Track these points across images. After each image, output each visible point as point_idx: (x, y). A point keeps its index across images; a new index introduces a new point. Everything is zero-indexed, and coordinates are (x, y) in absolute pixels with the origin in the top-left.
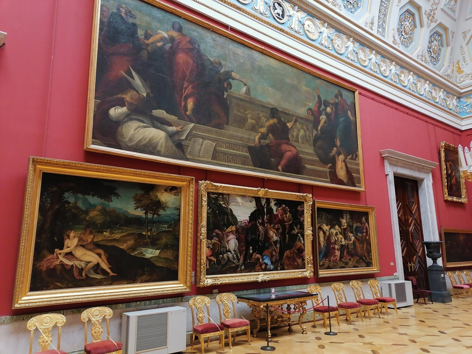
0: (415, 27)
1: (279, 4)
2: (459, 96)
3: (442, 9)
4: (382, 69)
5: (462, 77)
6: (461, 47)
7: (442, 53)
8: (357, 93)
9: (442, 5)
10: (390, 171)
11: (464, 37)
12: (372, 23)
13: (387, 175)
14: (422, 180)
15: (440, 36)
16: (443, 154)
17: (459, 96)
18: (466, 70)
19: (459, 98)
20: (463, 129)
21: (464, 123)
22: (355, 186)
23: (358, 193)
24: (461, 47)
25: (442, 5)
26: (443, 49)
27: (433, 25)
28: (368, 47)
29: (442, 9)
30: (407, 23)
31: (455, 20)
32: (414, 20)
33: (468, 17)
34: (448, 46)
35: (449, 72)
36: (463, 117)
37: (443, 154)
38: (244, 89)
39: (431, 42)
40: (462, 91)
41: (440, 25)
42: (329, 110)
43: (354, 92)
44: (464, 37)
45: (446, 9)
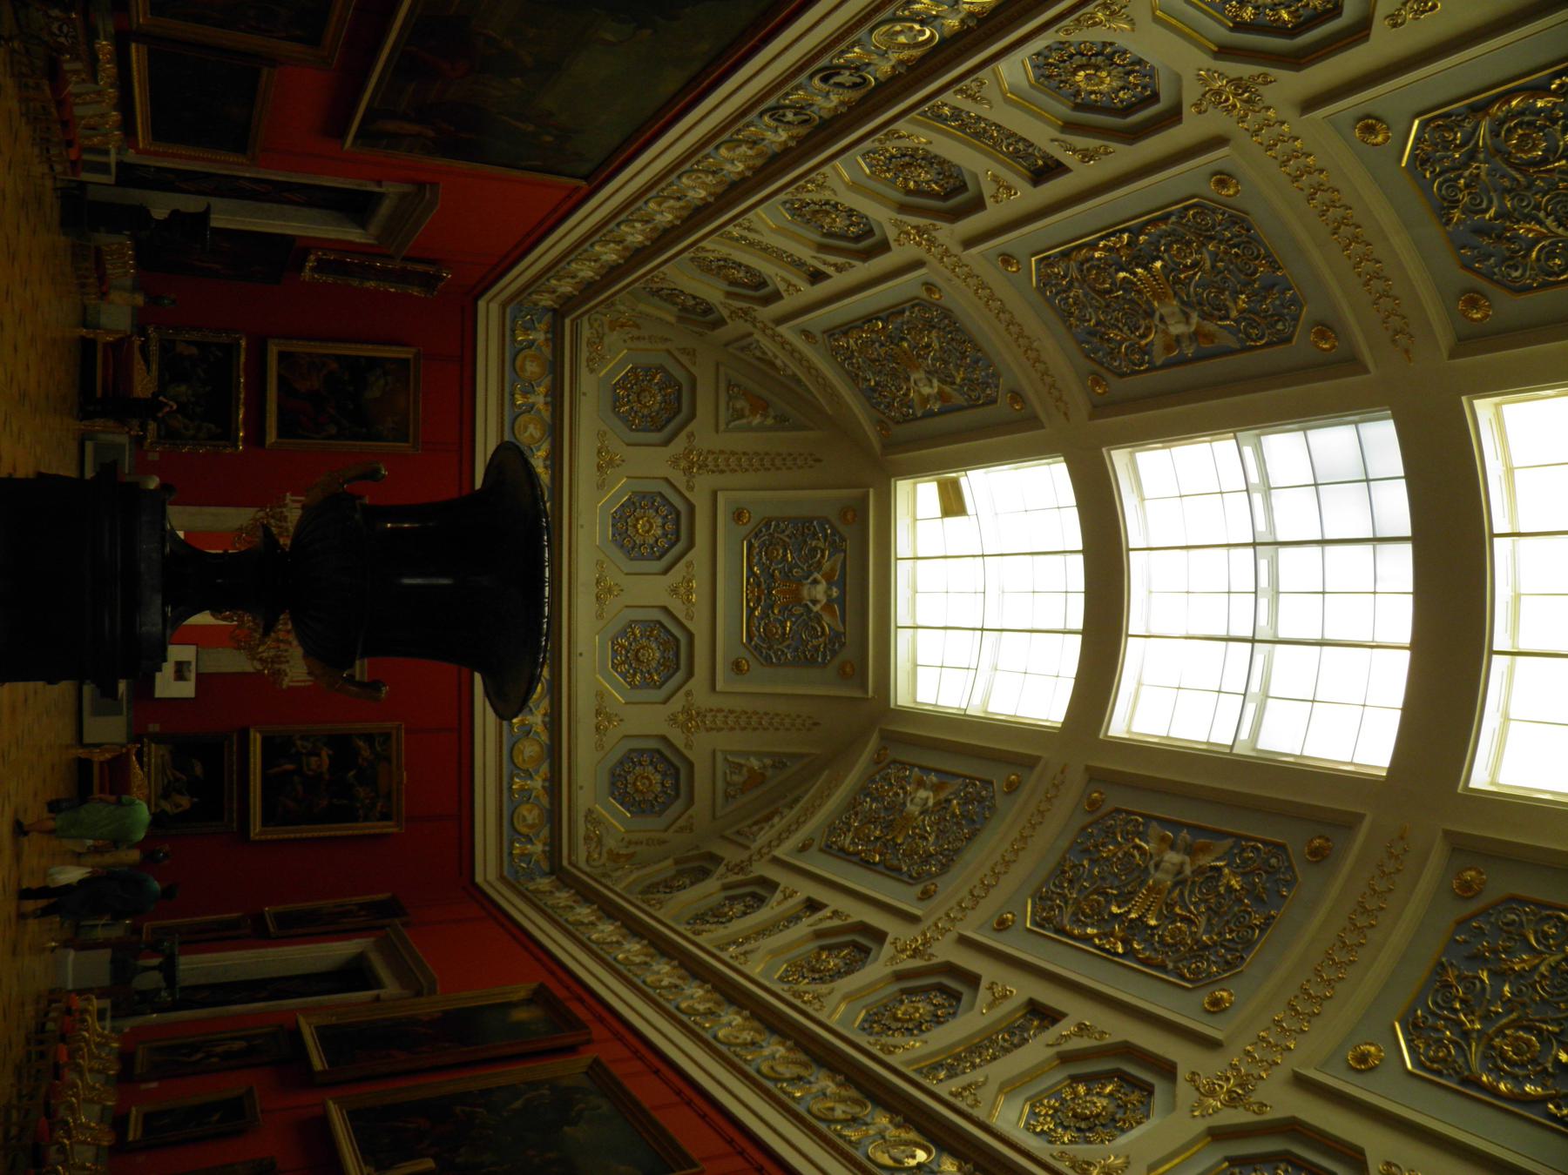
0: (733, 283)
1: (805, 122)
2: (558, 314)
3: (750, 334)
4: (638, 225)
5: (602, 325)
6: (666, 340)
7: (669, 306)
8: (583, 183)
9: (757, 336)
10: (391, 189)
11: (684, 351)
12: (749, 229)
13: (379, 183)
14: (363, 225)
15: (700, 315)
16: (420, 268)
17: (558, 314)
18: (613, 338)
19: (554, 310)
20: (481, 304)
21: (494, 307)
22: (356, 137)
23: (342, 135)
24: (666, 340)
25: (757, 336)
26: (675, 309)
27: (725, 313)
28: (690, 217)
29: (750, 334)
30: (742, 274)
31: (726, 345)
32: (744, 285)
33: (722, 369)
34: (680, 319)
35: (622, 308)
36: (508, 311)
37: (420, 268)
38: (609, 37)
39: (695, 298)
40: (567, 321)
41: (721, 322)
42: (549, 139)
43: (585, 178)
44: (684, 351)
45: (749, 340)
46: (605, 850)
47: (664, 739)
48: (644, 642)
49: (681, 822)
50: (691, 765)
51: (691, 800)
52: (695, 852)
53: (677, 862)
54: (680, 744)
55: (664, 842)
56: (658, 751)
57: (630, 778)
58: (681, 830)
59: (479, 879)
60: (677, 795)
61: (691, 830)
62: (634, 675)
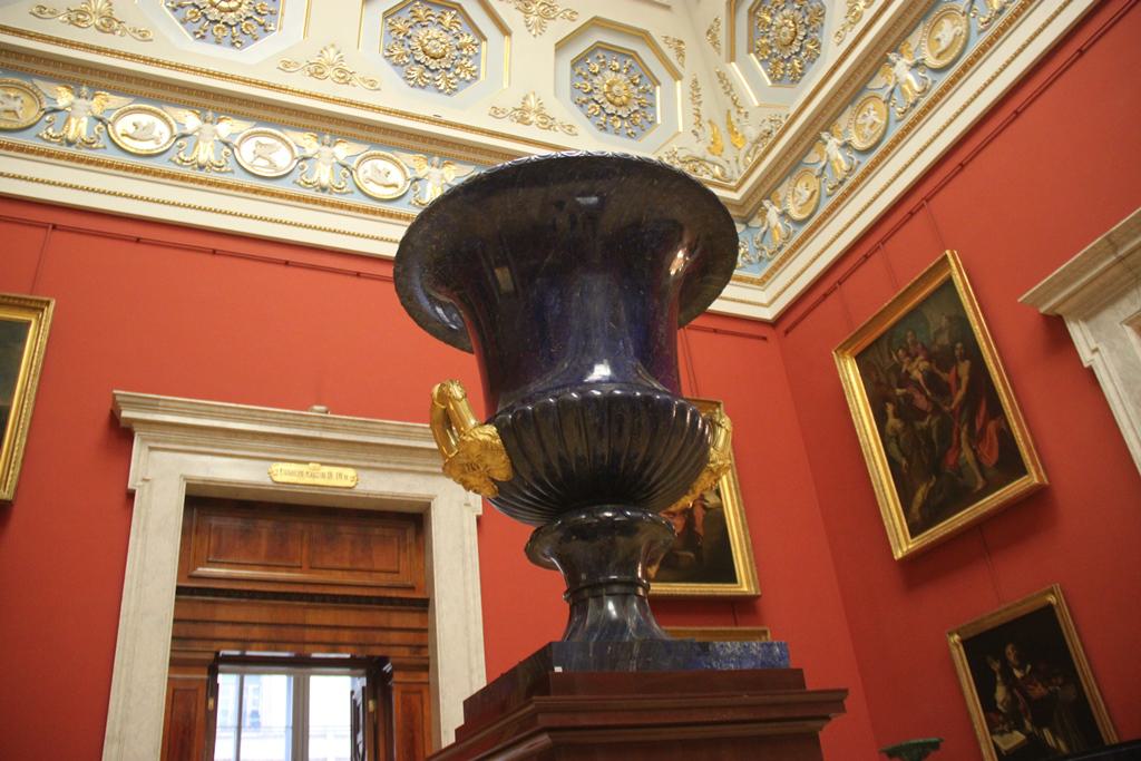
46: (709, 157)
47: (560, 46)
48: (415, 44)
49: (671, 54)
50: (596, 23)
51: (643, 36)
52: (722, 36)
53: (732, 58)
54: (571, 27)
55: (695, 82)
56: (575, 64)
57: (611, 109)
58: (681, 54)
59: (768, 314)
60: (633, 55)
61: (681, 42)
62: (462, 67)
